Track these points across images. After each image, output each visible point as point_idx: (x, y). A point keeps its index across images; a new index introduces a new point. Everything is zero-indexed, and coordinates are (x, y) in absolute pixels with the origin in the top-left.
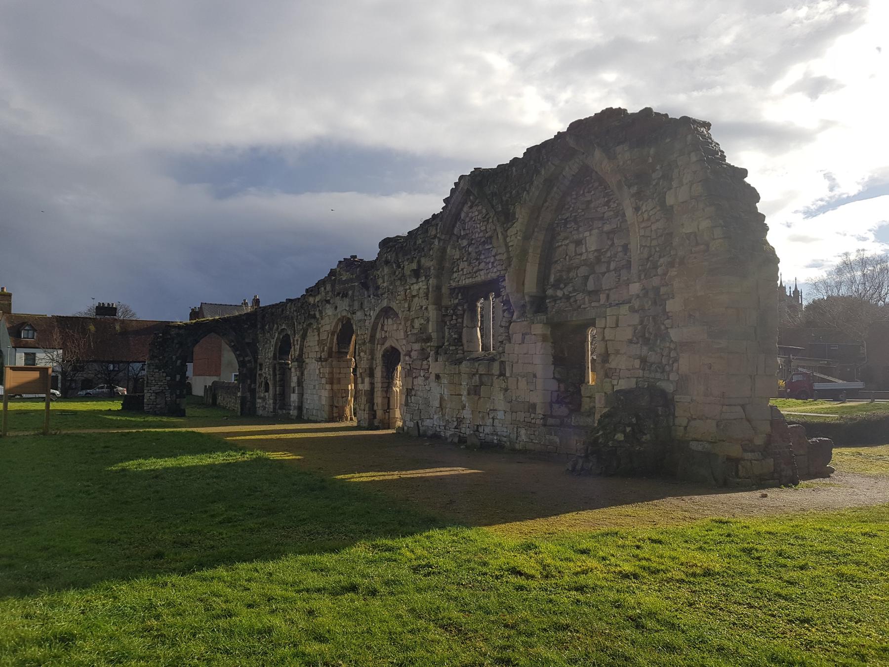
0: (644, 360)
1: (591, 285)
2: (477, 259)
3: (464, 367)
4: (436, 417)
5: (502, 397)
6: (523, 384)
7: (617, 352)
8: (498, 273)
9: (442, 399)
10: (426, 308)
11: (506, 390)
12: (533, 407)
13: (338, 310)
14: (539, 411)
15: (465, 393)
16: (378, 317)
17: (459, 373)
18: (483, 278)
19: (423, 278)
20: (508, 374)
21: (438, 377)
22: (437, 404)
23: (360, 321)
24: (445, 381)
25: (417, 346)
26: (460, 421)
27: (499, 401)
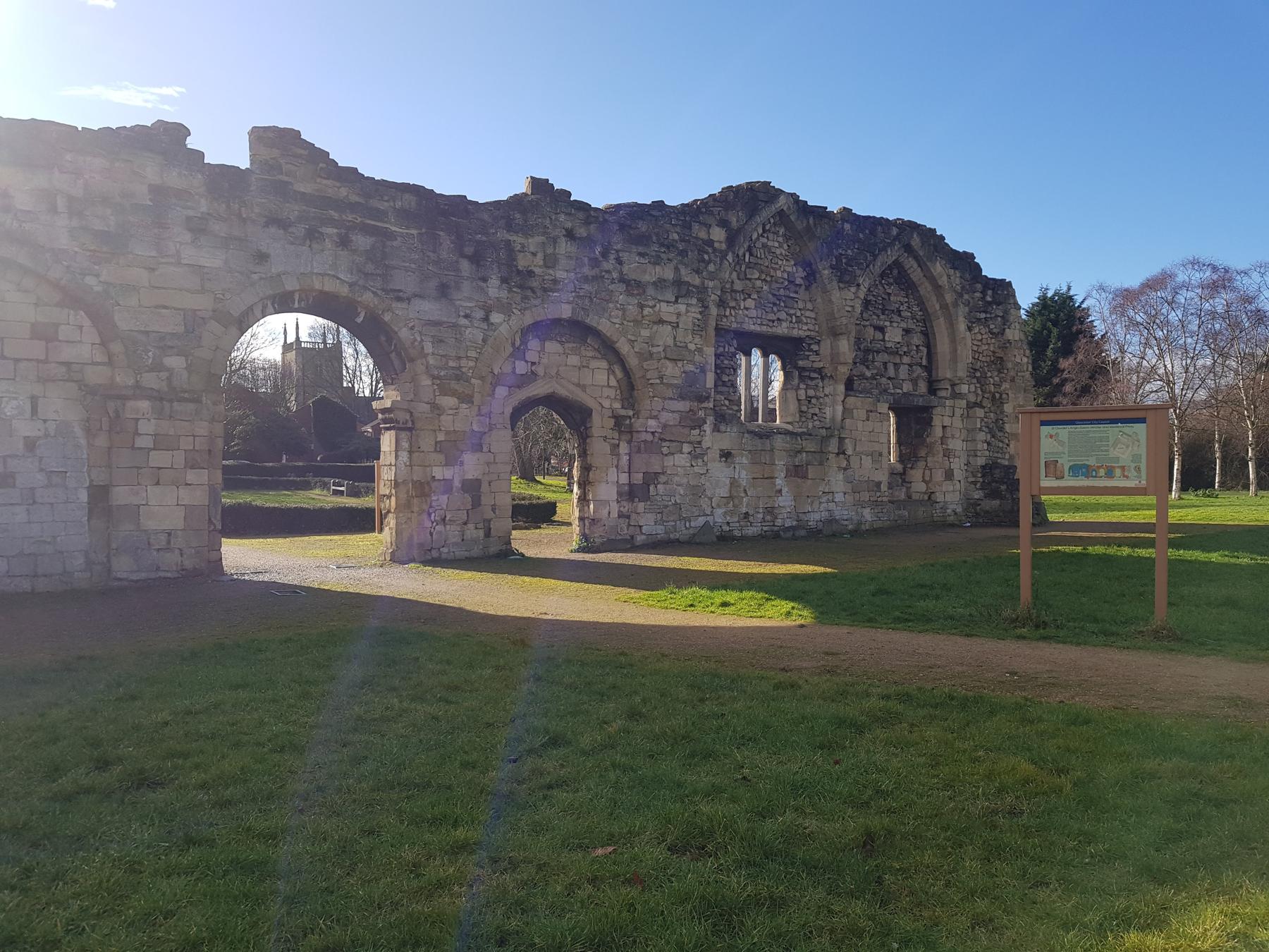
0: (989, 444)
1: (891, 372)
2: (774, 304)
3: (779, 441)
4: (719, 512)
5: (841, 476)
6: (867, 462)
7: (953, 437)
8: (808, 333)
9: (734, 483)
10: (700, 350)
11: (845, 469)
12: (879, 484)
14: (884, 487)
15: (783, 475)
16: (526, 332)
17: (772, 450)
18: (786, 331)
19: (694, 301)
20: (849, 452)
22: (724, 492)
23: (437, 324)
25: (683, 406)
26: (770, 511)
27: (837, 482)
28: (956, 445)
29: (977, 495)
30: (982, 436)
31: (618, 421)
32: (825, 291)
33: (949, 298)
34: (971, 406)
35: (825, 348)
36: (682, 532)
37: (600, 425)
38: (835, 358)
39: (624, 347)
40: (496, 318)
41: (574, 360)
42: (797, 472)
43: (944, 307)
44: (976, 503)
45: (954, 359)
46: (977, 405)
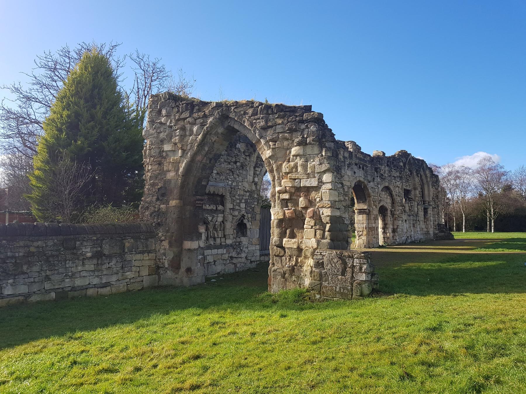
13: (356, 175)
21: (406, 221)
24: (407, 222)
28: (432, 218)
29: (437, 232)
30: (437, 216)
31: (391, 211)
32: (414, 178)
33: (429, 179)
34: (433, 208)
35: (413, 193)
36: (401, 242)
37: (389, 212)
38: (415, 196)
39: (394, 193)
40: (379, 186)
41: (386, 196)
42: (414, 226)
43: (427, 182)
44: (436, 234)
45: (429, 195)
46: (435, 208)
